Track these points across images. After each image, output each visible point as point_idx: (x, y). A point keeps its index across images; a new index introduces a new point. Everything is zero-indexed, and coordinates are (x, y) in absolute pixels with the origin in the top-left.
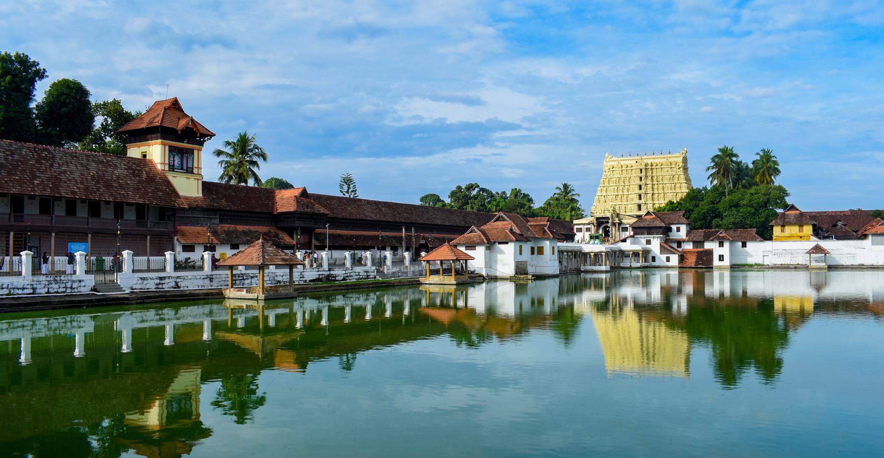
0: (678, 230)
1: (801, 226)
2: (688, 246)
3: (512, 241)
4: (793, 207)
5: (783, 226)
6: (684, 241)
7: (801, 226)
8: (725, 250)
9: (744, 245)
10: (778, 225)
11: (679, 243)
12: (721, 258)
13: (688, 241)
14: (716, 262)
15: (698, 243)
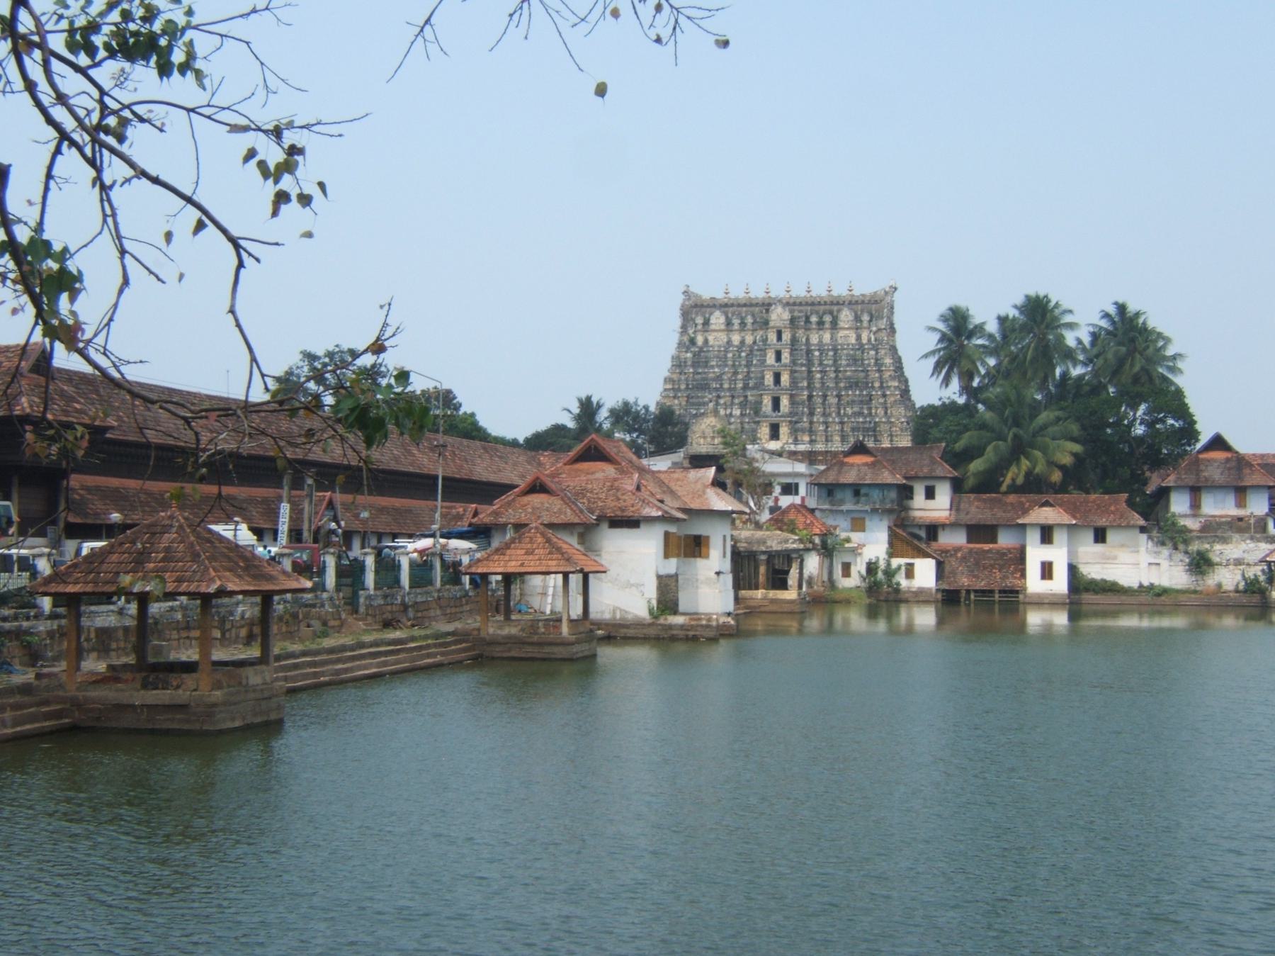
0: (930, 494)
1: (1241, 492)
2: (956, 539)
3: (651, 520)
4: (1218, 443)
5: (1195, 491)
6: (944, 526)
7: (1241, 492)
8: (1058, 554)
9: (1100, 536)
10: (1178, 488)
11: (933, 530)
12: (1047, 571)
13: (954, 525)
14: (1034, 583)
15: (981, 532)
